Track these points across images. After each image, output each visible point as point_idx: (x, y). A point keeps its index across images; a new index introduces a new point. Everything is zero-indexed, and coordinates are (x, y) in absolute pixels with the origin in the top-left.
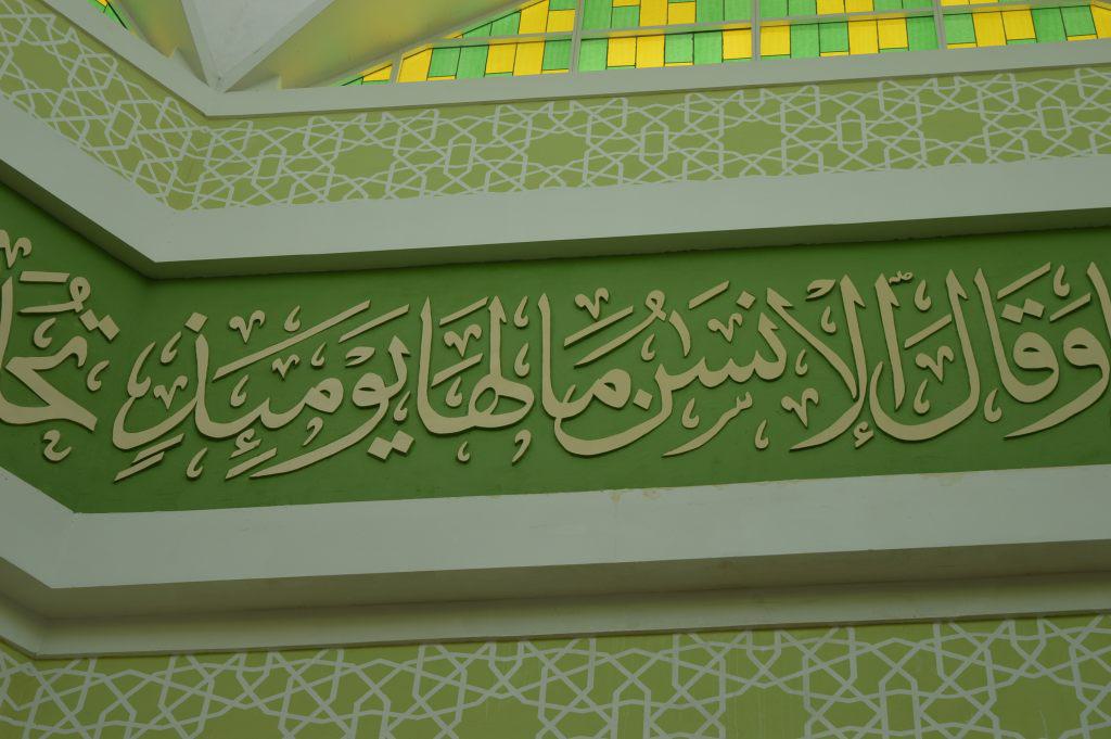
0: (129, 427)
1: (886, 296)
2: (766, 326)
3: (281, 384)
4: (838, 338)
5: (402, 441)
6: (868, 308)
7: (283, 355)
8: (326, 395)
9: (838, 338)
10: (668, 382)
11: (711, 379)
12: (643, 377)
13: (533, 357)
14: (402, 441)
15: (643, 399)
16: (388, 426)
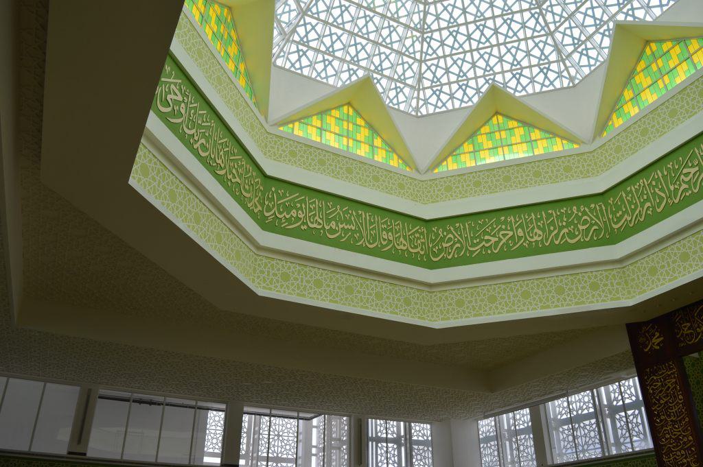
0: (267, 212)
1: (368, 218)
2: (353, 218)
3: (288, 209)
4: (362, 224)
5: (305, 227)
6: (366, 219)
7: (287, 201)
8: (294, 213)
9: (362, 224)
10: (341, 226)
11: (346, 227)
12: (337, 225)
13: (322, 215)
14: (305, 227)
15: (337, 228)
16: (303, 223)
